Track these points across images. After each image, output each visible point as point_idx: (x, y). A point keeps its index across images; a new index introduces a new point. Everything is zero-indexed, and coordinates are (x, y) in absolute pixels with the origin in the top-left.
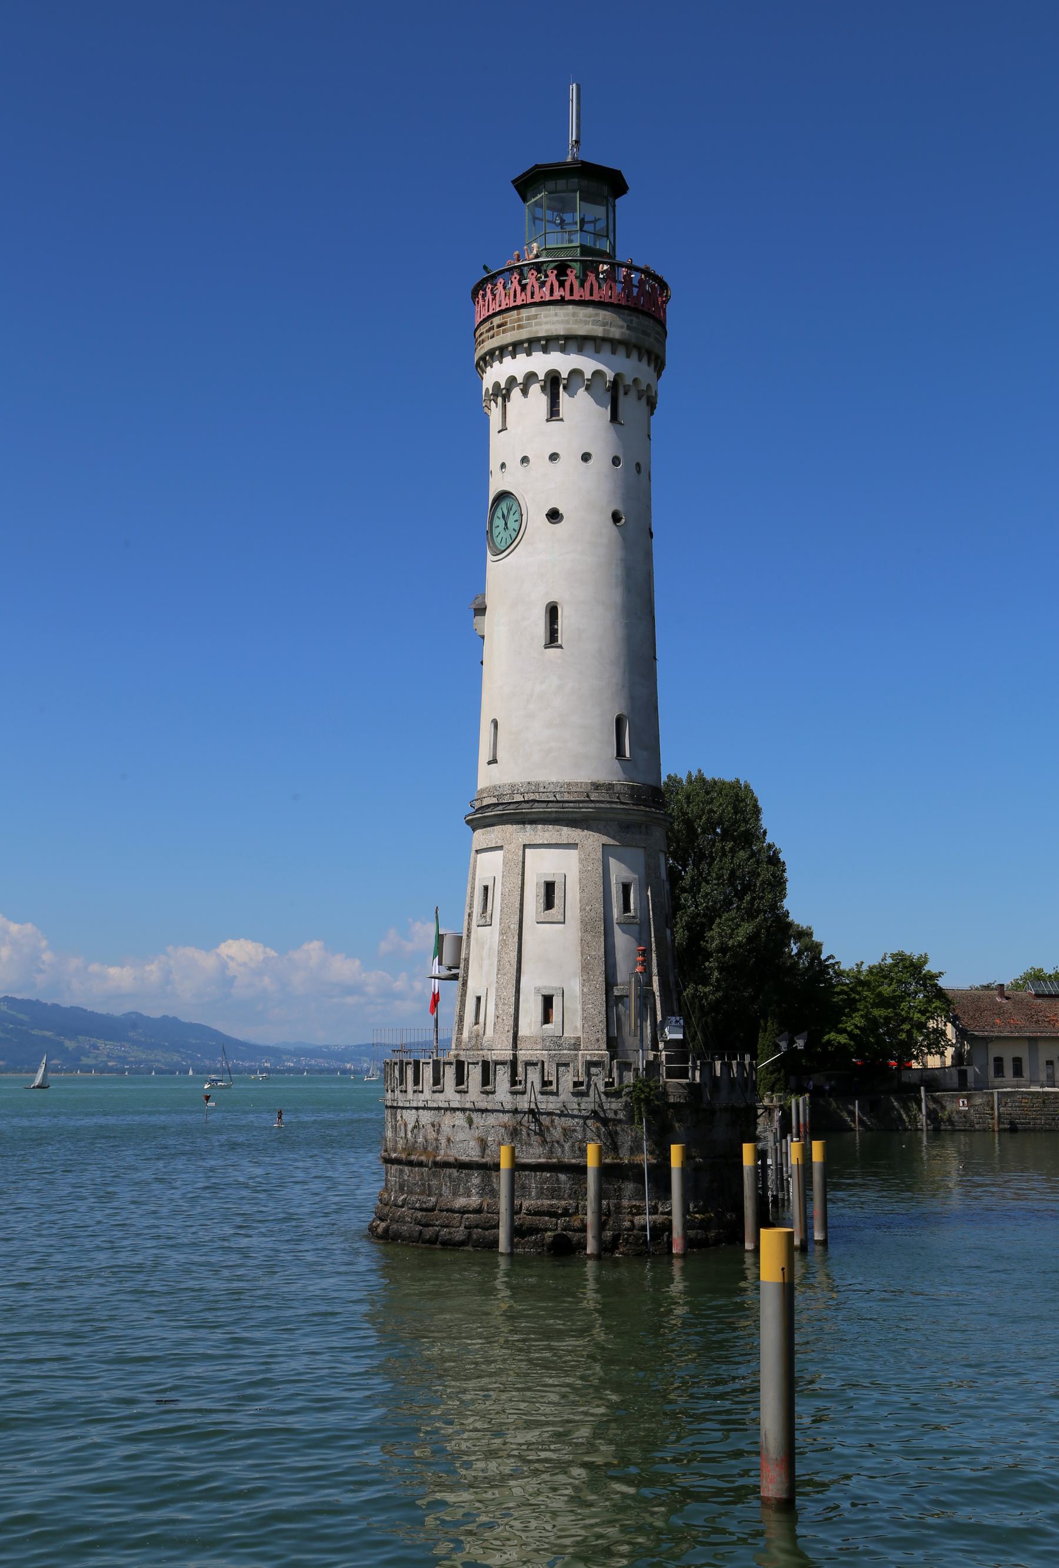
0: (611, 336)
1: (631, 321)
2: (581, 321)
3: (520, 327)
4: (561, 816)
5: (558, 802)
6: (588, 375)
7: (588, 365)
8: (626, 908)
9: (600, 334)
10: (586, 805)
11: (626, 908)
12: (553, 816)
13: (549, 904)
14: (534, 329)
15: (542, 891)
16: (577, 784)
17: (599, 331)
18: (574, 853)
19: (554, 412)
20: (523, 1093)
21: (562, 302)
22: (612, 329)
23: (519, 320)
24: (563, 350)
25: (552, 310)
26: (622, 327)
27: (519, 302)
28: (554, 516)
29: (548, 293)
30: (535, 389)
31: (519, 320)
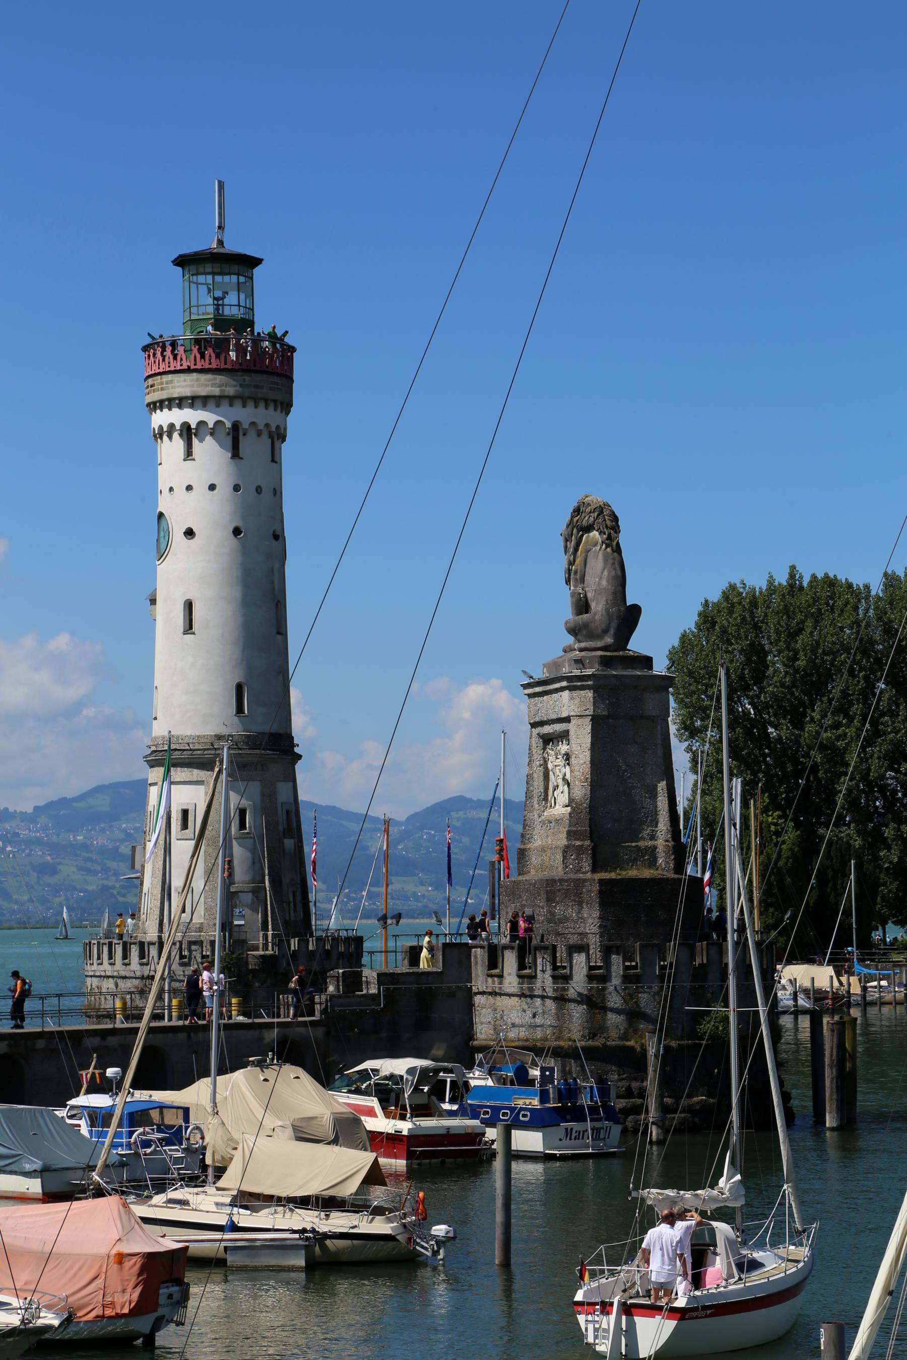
0: (226, 394)
1: (244, 380)
2: (202, 385)
3: (162, 389)
4: (192, 760)
5: (191, 750)
6: (211, 425)
7: (210, 418)
8: (242, 825)
9: (217, 394)
10: (209, 752)
11: (242, 825)
12: (187, 760)
13: (185, 826)
14: (171, 391)
15: (180, 816)
16: (204, 736)
17: (216, 391)
18: (202, 788)
19: (189, 453)
20: (147, 964)
21: (189, 370)
22: (228, 389)
23: (162, 383)
24: (192, 406)
25: (182, 376)
26: (236, 386)
27: (161, 370)
28: (189, 533)
29: (179, 363)
30: (176, 435)
31: (162, 383)
